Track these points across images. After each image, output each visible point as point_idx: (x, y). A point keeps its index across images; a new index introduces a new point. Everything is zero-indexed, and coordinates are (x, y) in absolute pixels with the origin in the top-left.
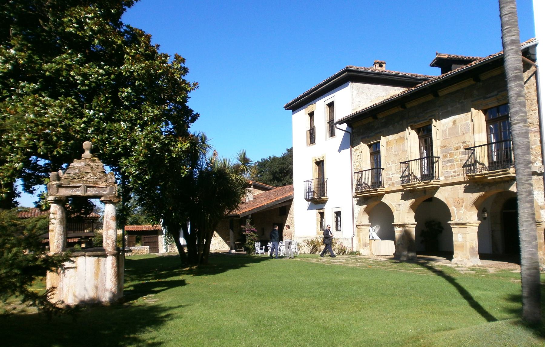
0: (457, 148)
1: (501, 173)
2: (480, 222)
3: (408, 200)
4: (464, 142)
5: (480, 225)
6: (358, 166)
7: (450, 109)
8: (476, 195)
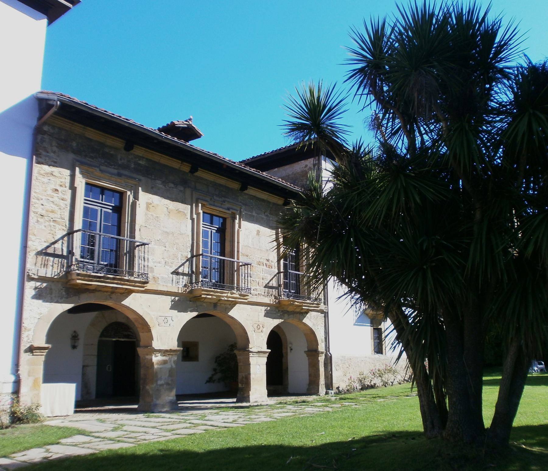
0: (259, 264)
1: (314, 305)
2: (270, 351)
3: (185, 310)
4: (268, 260)
5: (270, 353)
6: (52, 212)
7: (254, 214)
8: (277, 322)
